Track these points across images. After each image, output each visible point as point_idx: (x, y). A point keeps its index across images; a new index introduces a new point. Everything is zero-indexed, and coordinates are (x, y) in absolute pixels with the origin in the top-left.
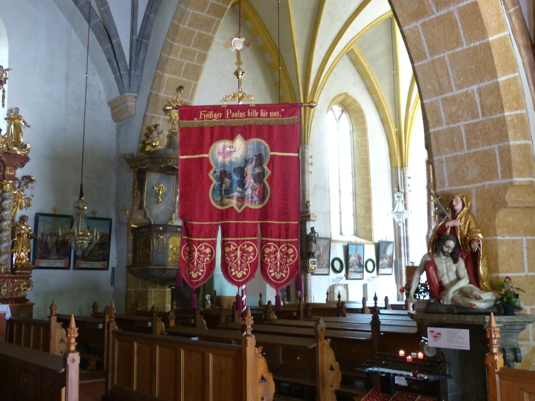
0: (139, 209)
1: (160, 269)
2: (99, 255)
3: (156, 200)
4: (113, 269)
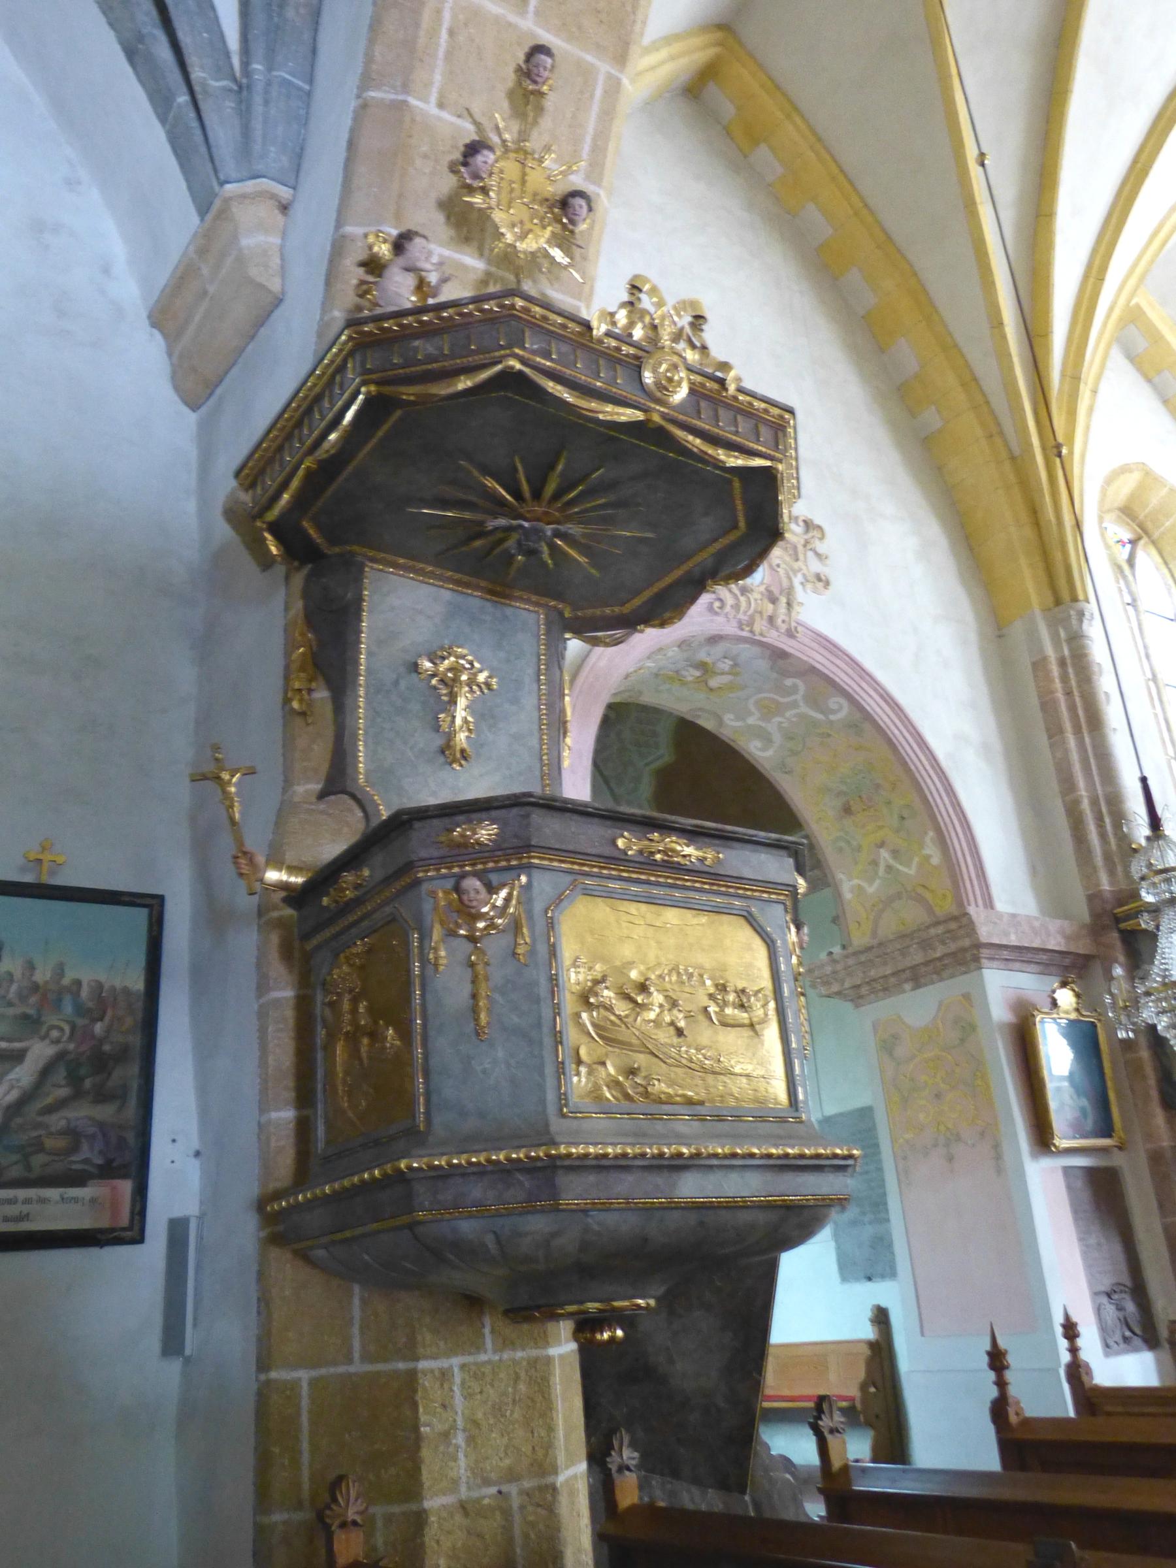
0: (322, 795)
1: (506, 1171)
2: (74, 1135)
3: (439, 741)
4: (177, 1230)
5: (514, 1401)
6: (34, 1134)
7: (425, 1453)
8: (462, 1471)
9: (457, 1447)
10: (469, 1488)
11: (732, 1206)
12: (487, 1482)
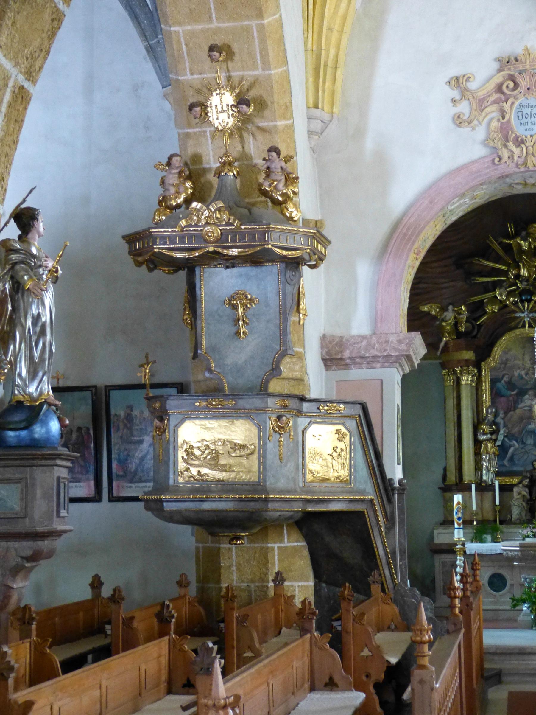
5: (254, 559)
7: (222, 571)
8: (235, 578)
9: (233, 571)
10: (237, 583)
12: (243, 582)
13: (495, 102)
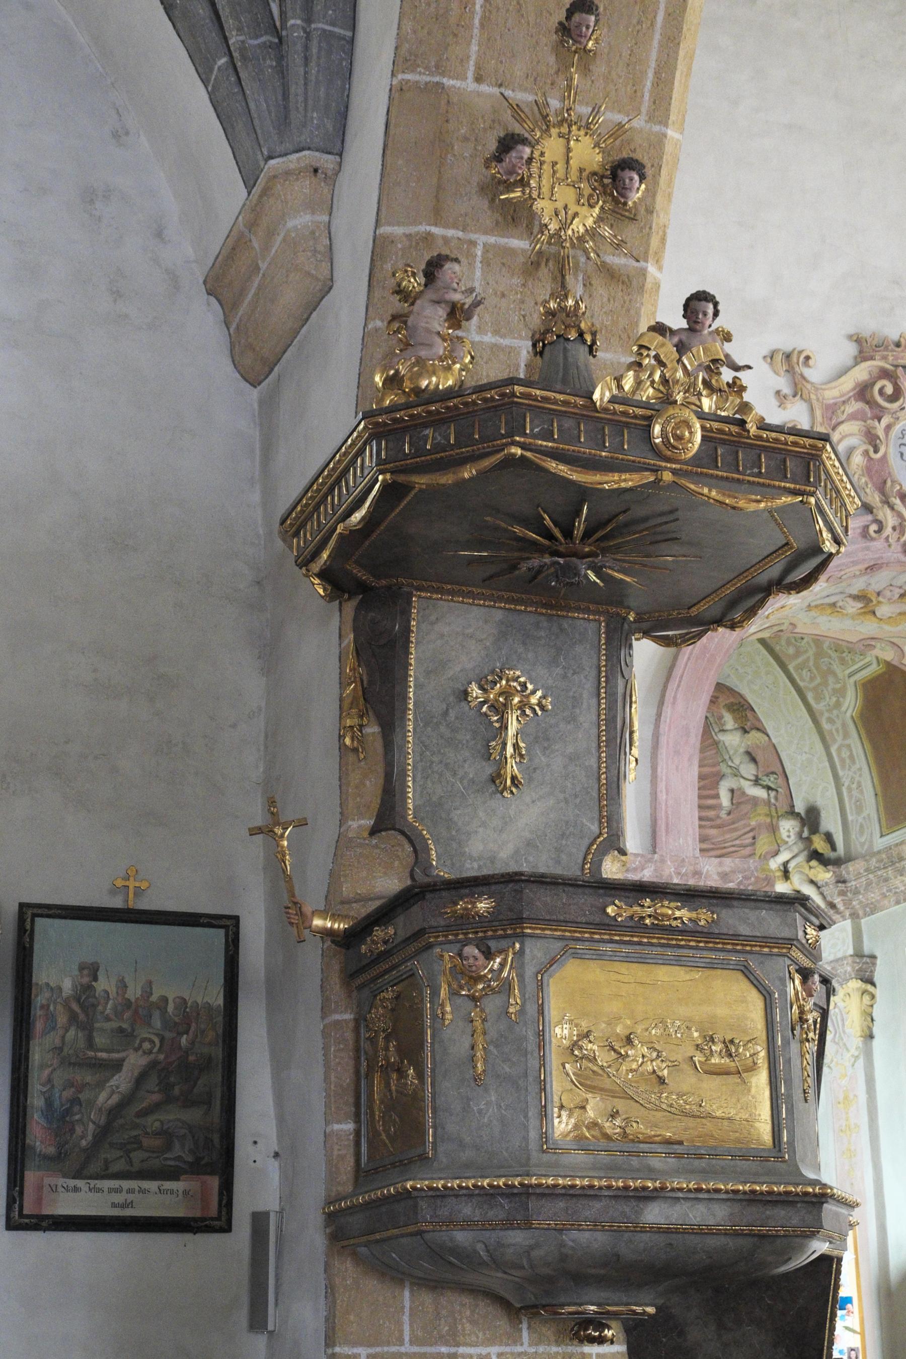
0: (373, 832)
1: (492, 1194)
2: (167, 1136)
4: (259, 1221)
6: (134, 1133)
11: (700, 1231)
13: (853, 417)
